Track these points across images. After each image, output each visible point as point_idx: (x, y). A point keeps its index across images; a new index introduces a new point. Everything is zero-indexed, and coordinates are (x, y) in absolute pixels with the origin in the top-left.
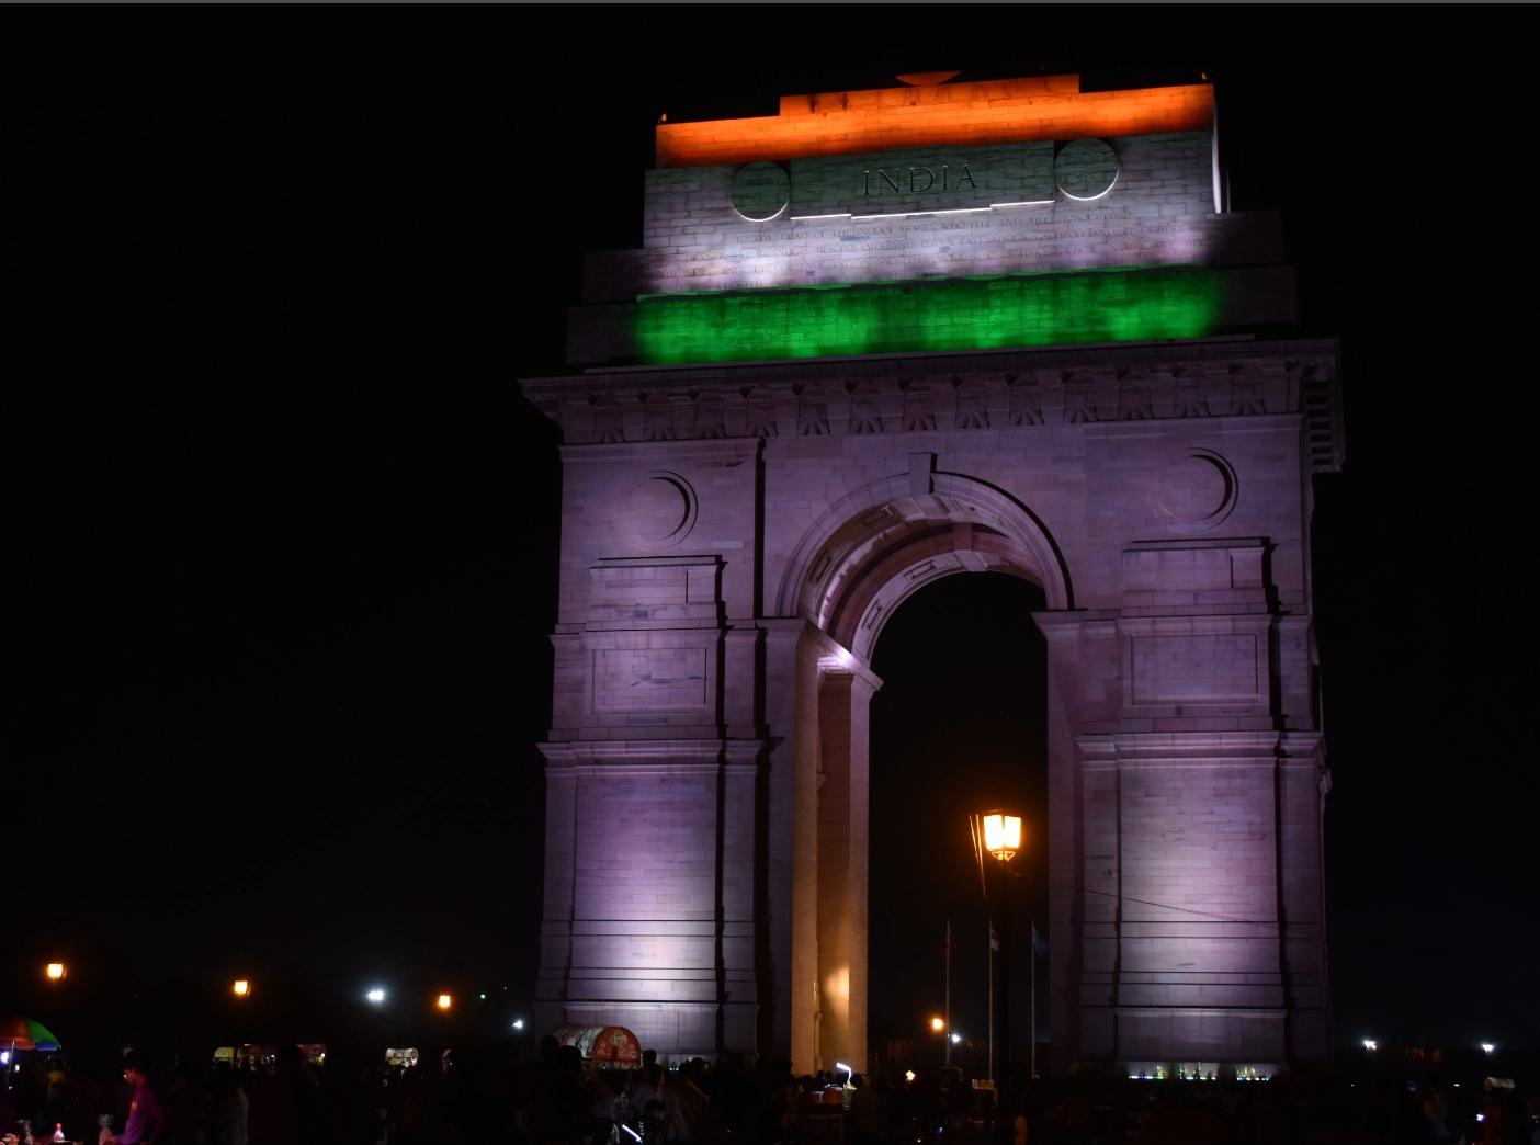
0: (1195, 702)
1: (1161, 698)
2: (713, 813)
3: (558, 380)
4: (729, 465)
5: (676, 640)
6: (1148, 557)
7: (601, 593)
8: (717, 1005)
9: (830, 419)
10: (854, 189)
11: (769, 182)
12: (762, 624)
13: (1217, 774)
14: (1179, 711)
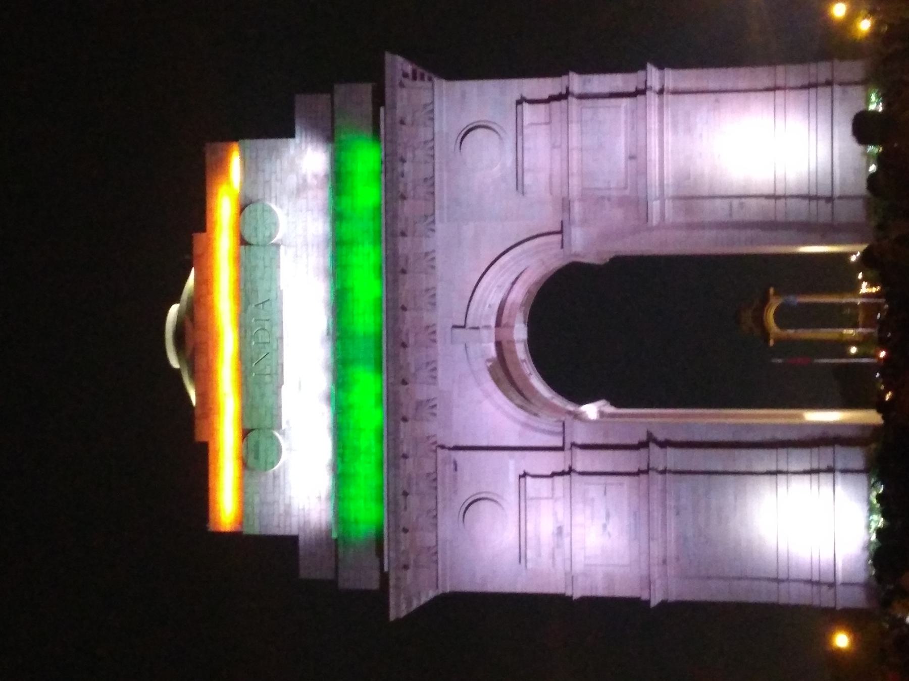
0: (626, 146)
1: (623, 170)
3: (392, 591)
4: (456, 469)
5: (578, 507)
6: (528, 179)
10: (266, 384)
11: (257, 445)
12: (568, 446)
14: (632, 157)
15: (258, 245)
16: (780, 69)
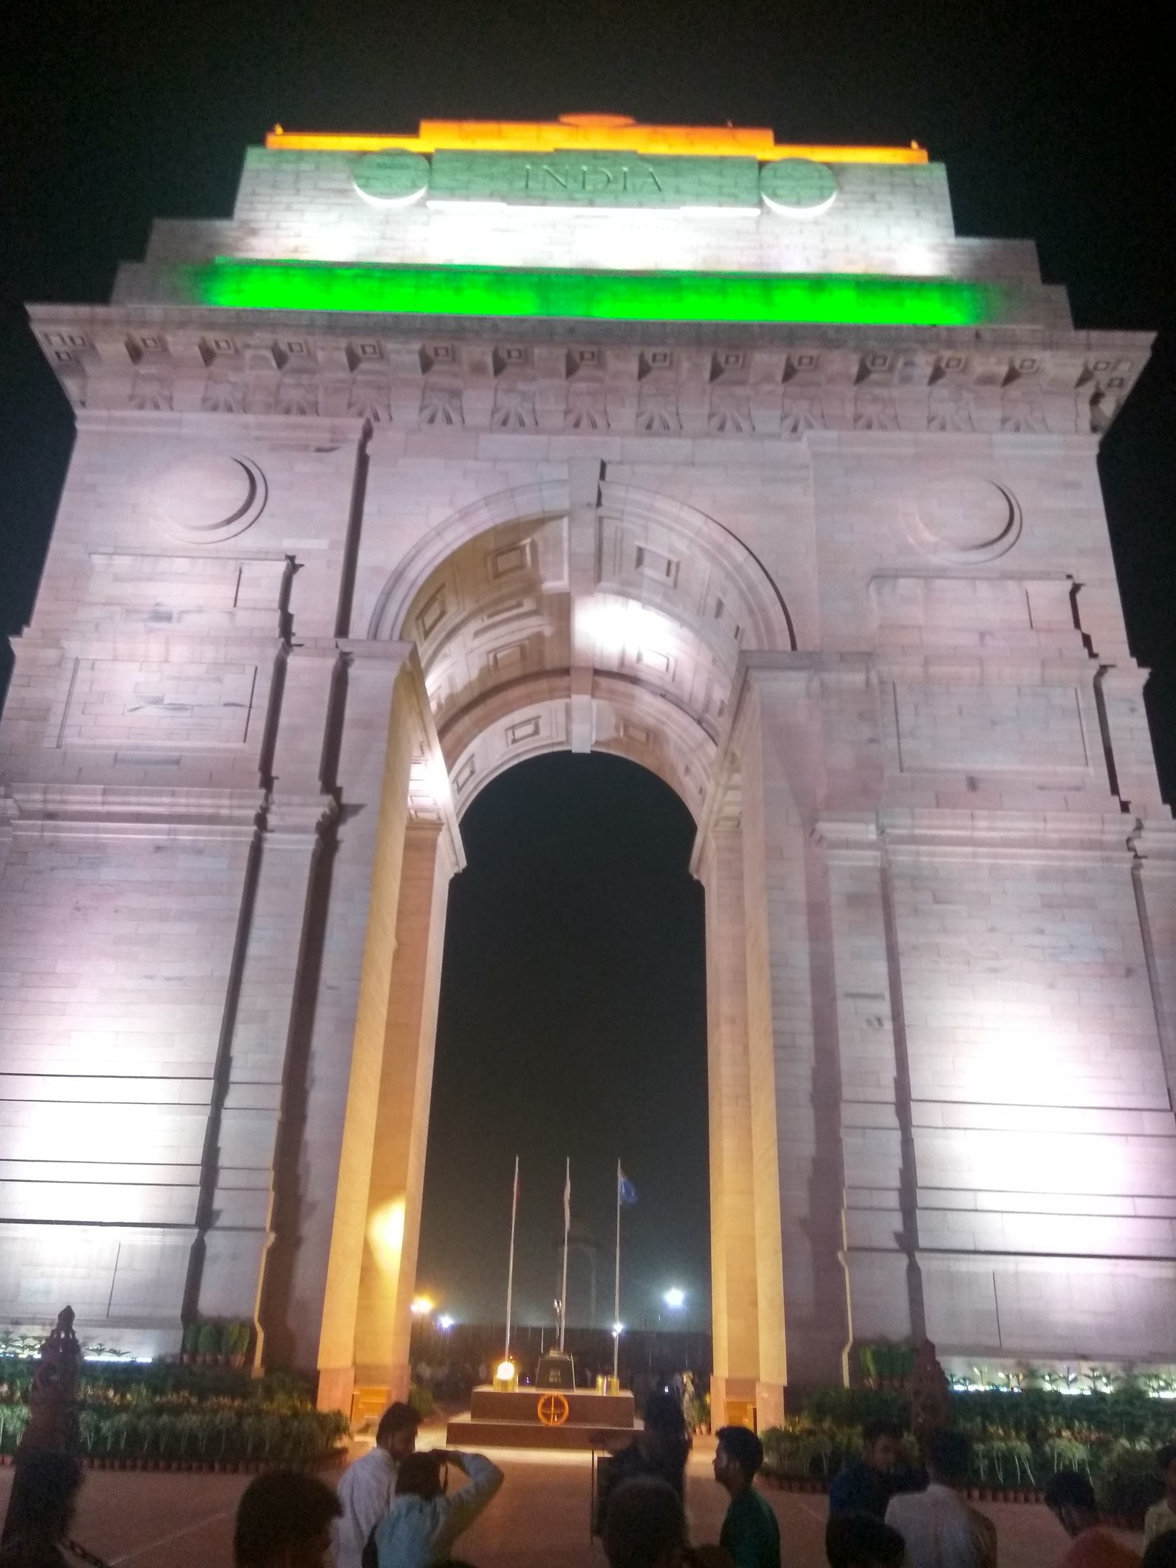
2: (238, 902)
3: (84, 310)
4: (319, 450)
5: (209, 653)
7: (101, 587)
9: (465, 406)
11: (404, 167)
13: (1043, 875)
14: (973, 783)
15: (759, 178)
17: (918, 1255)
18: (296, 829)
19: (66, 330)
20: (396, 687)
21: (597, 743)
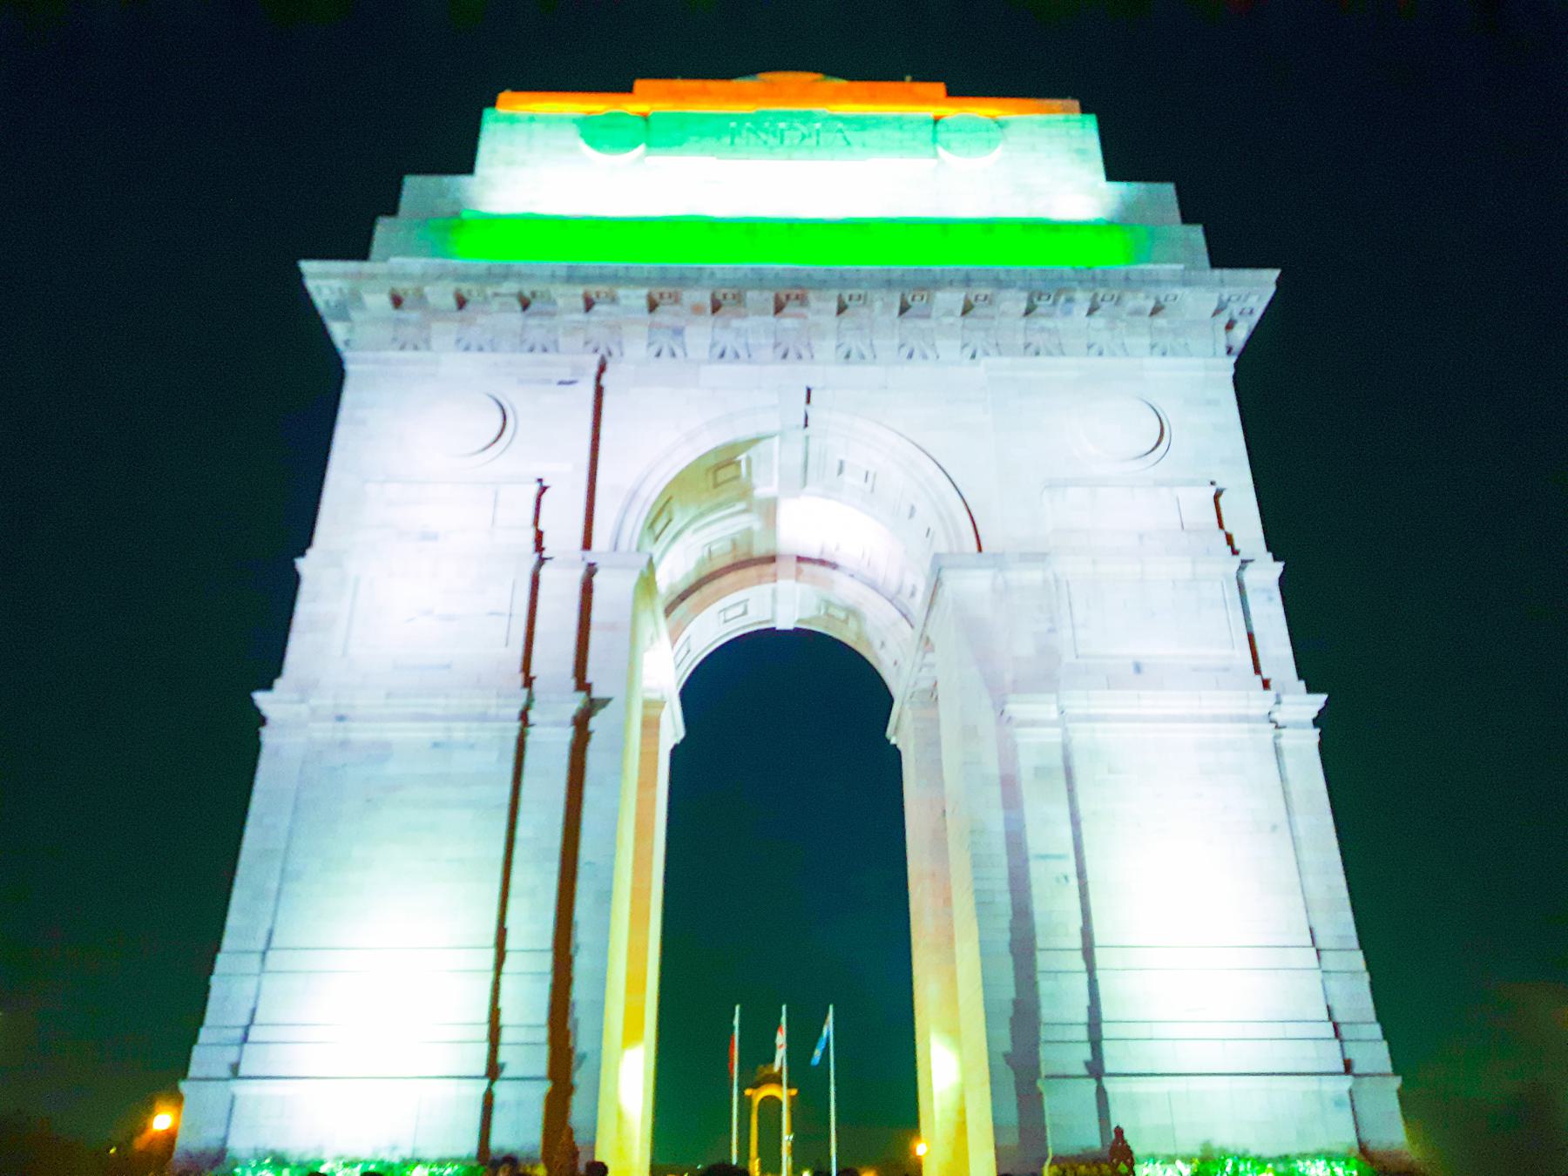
3: (352, 266)
4: (561, 383)
8: (486, 1082)
12: (590, 557)
14: (1138, 668)
15: (935, 132)
16: (1358, 960)
17: (1105, 1080)
18: (557, 724)
19: (336, 283)
20: (635, 592)
21: (799, 621)
